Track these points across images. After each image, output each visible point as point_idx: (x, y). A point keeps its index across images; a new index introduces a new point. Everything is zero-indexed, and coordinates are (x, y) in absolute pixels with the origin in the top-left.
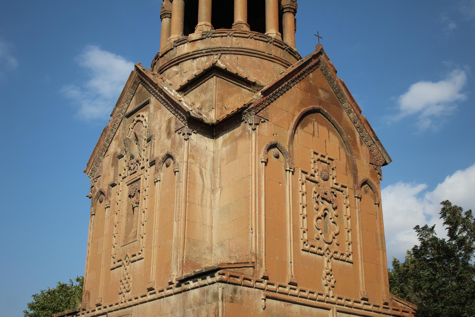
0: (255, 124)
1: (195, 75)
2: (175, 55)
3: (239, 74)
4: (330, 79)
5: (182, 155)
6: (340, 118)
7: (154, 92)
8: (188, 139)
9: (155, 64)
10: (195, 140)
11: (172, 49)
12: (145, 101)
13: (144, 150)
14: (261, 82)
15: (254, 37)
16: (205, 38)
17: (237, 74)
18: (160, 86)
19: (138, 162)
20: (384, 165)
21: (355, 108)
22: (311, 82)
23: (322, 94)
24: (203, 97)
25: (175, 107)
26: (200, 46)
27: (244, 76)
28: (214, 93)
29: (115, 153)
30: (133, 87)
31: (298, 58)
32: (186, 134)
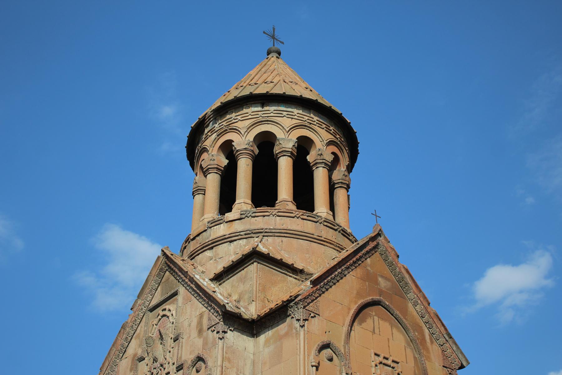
0: (304, 320)
1: (233, 261)
2: (208, 238)
4: (391, 265)
5: (215, 359)
6: (405, 311)
7: (183, 281)
8: (223, 337)
9: (185, 248)
10: (232, 339)
11: (205, 230)
12: (173, 292)
13: (170, 352)
14: (309, 269)
15: (302, 217)
16: (244, 218)
17: (281, 259)
18: (190, 275)
19: (162, 365)
20: (460, 368)
21: (422, 299)
22: (369, 268)
23: (383, 283)
24: (241, 288)
25: (208, 299)
26: (238, 227)
27: (290, 262)
28: (255, 282)
29: (135, 355)
30: (159, 274)
31: (353, 240)
32: (221, 332)
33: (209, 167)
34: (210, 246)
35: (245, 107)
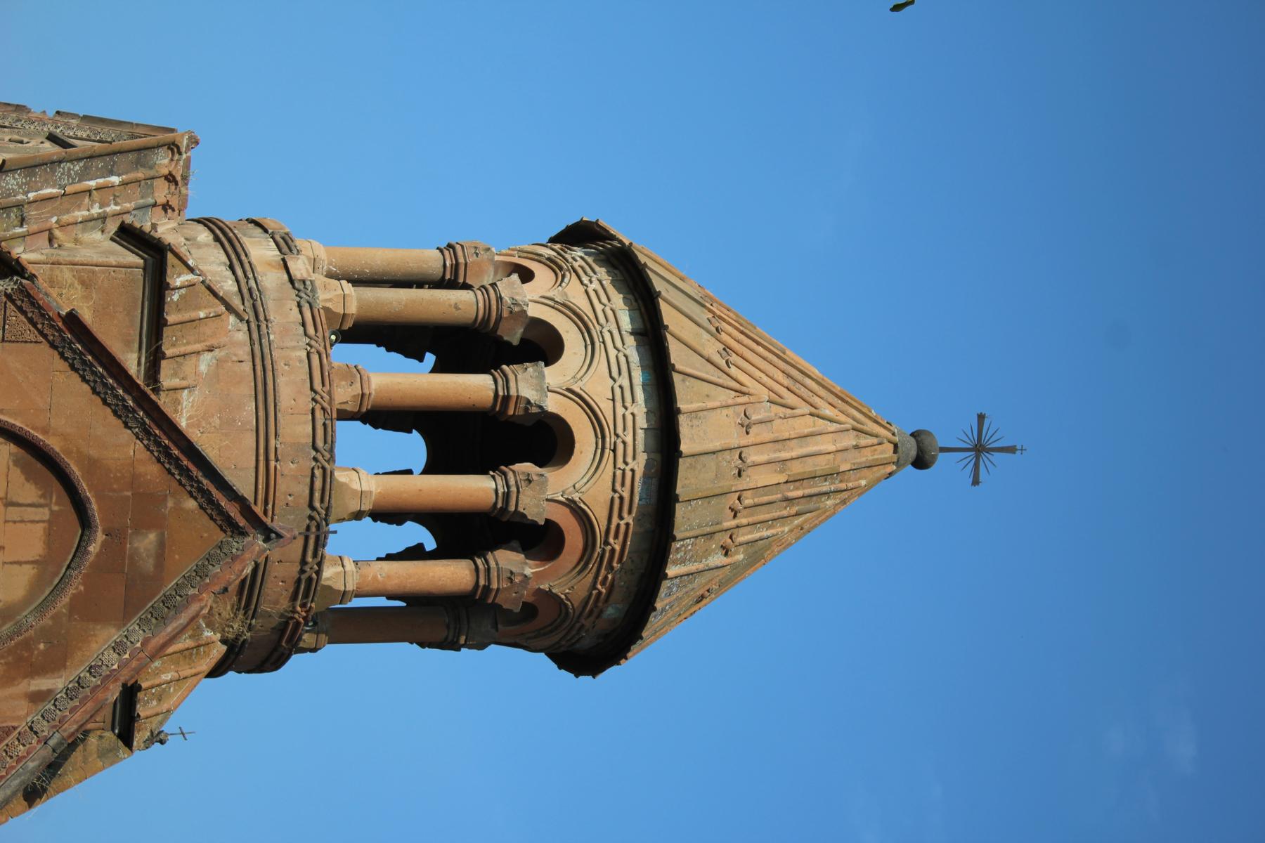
3: (167, 331)
6: (89, 610)
11: (266, 231)
15: (318, 407)
16: (294, 287)
21: (134, 664)
22: (170, 504)
26: (271, 279)
33: (458, 248)
34: (221, 235)
35: (630, 297)
